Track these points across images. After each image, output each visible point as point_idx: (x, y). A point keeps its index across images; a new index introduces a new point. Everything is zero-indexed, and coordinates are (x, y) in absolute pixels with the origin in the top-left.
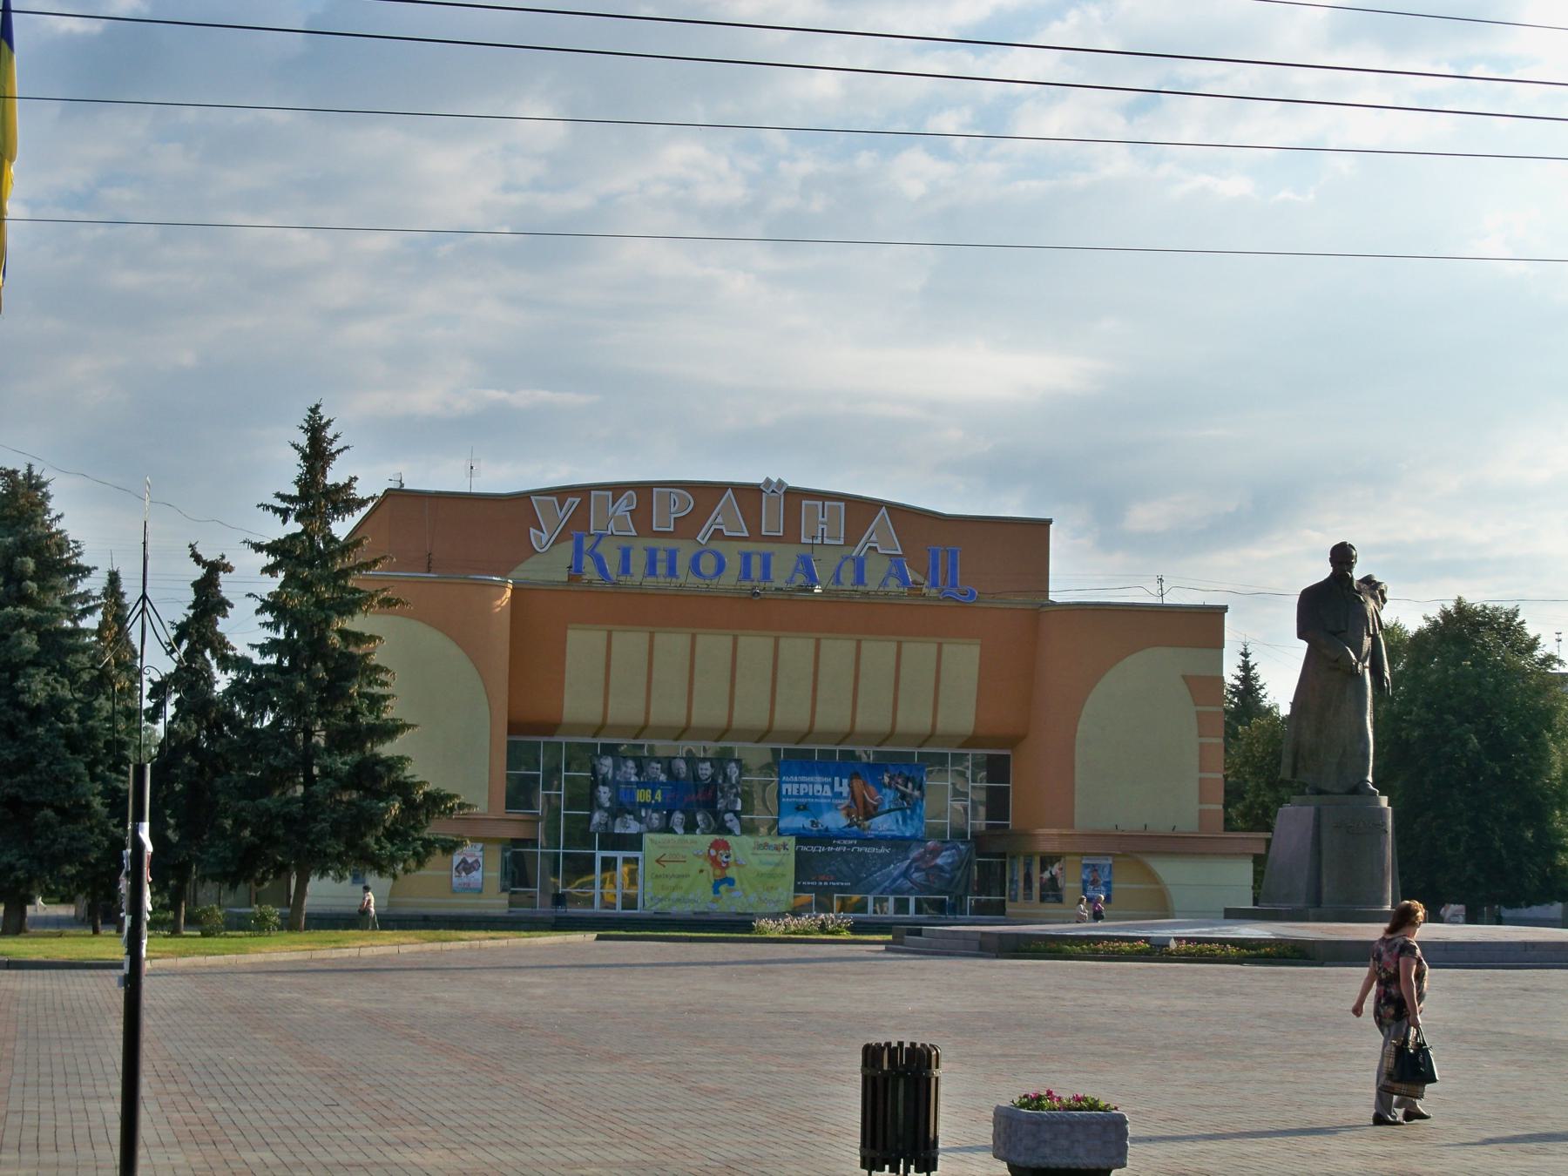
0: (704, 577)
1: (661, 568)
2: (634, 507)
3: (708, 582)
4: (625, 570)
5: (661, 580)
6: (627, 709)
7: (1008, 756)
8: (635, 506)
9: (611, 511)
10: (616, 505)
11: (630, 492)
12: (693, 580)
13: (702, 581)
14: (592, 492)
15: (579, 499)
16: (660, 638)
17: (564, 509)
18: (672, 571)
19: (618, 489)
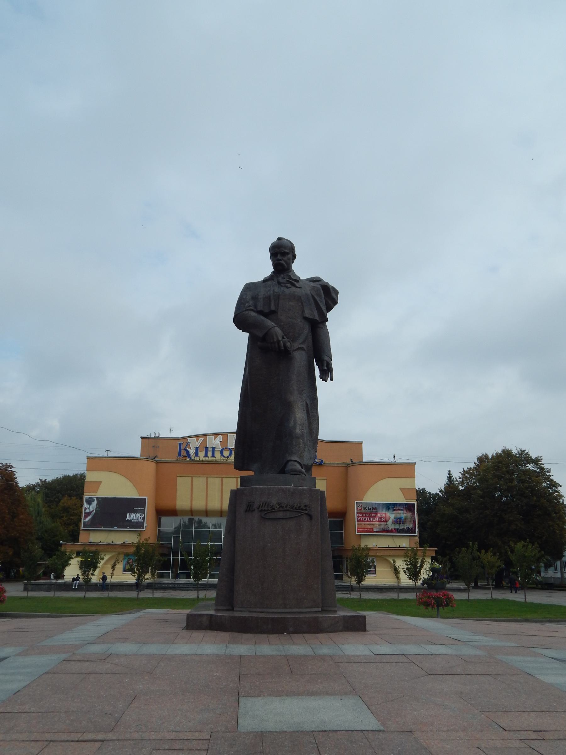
0: (225, 457)
1: (210, 454)
2: (221, 441)
3: (227, 459)
4: (197, 454)
5: (210, 458)
6: (199, 504)
7: (342, 521)
8: (222, 439)
9: (213, 442)
10: (216, 440)
11: (220, 436)
12: (222, 459)
13: (224, 458)
14: (208, 436)
15: (203, 439)
16: (209, 479)
17: (198, 442)
18: (213, 455)
19: (216, 435)
